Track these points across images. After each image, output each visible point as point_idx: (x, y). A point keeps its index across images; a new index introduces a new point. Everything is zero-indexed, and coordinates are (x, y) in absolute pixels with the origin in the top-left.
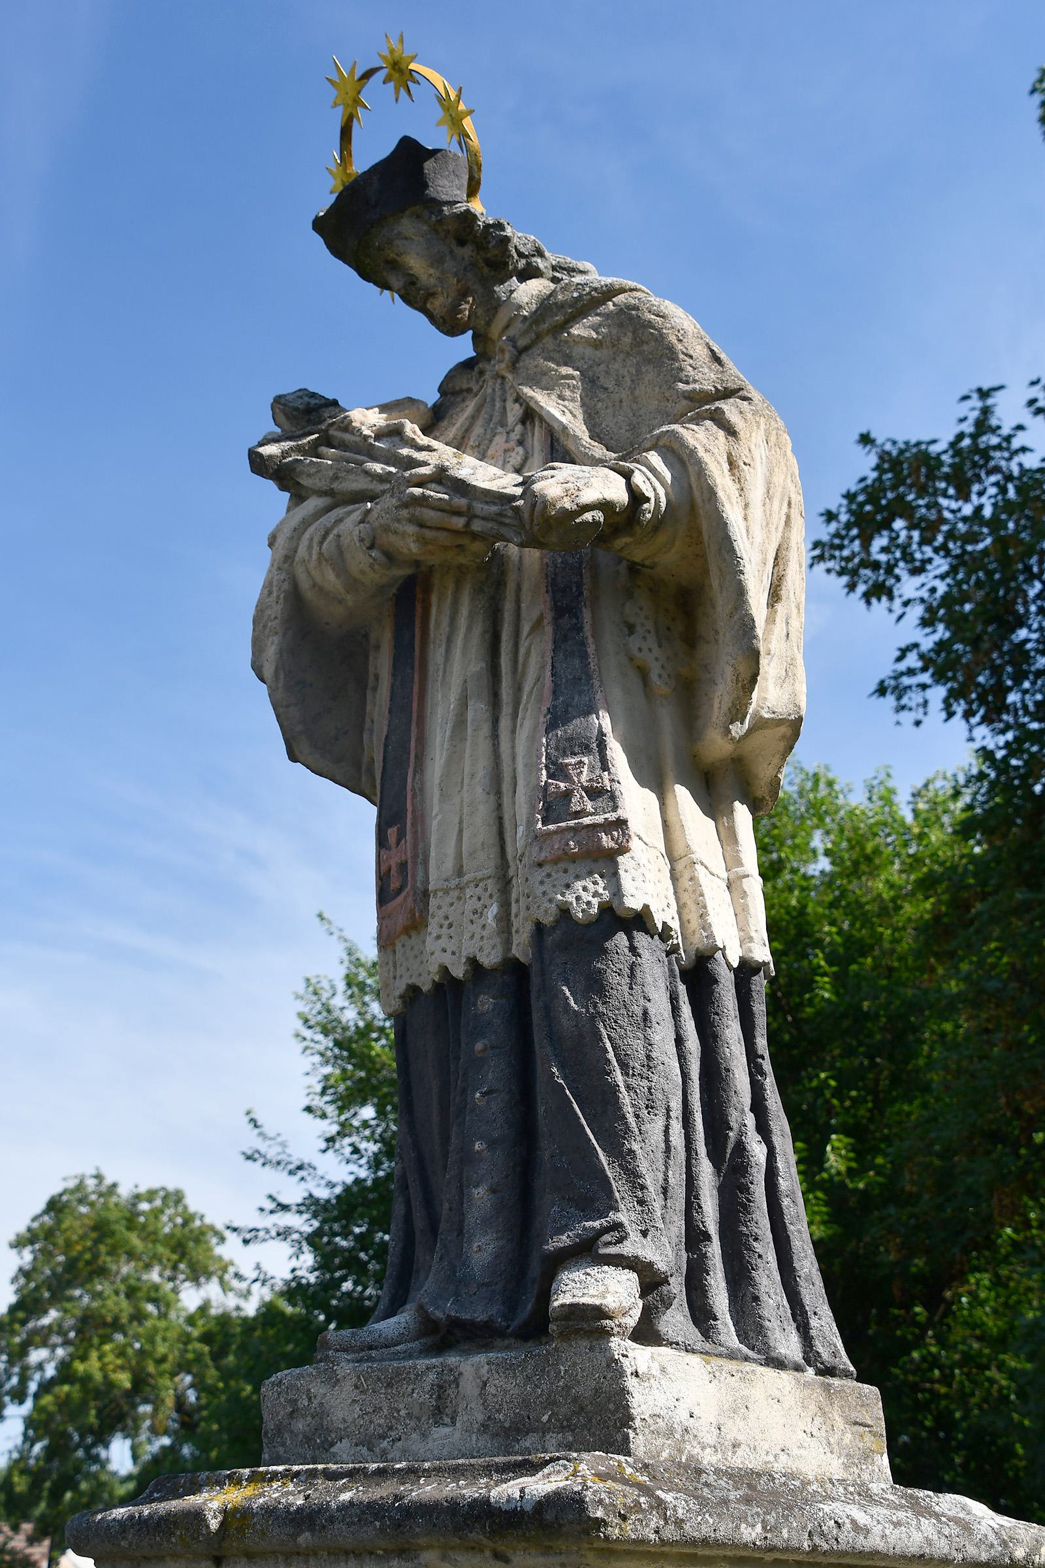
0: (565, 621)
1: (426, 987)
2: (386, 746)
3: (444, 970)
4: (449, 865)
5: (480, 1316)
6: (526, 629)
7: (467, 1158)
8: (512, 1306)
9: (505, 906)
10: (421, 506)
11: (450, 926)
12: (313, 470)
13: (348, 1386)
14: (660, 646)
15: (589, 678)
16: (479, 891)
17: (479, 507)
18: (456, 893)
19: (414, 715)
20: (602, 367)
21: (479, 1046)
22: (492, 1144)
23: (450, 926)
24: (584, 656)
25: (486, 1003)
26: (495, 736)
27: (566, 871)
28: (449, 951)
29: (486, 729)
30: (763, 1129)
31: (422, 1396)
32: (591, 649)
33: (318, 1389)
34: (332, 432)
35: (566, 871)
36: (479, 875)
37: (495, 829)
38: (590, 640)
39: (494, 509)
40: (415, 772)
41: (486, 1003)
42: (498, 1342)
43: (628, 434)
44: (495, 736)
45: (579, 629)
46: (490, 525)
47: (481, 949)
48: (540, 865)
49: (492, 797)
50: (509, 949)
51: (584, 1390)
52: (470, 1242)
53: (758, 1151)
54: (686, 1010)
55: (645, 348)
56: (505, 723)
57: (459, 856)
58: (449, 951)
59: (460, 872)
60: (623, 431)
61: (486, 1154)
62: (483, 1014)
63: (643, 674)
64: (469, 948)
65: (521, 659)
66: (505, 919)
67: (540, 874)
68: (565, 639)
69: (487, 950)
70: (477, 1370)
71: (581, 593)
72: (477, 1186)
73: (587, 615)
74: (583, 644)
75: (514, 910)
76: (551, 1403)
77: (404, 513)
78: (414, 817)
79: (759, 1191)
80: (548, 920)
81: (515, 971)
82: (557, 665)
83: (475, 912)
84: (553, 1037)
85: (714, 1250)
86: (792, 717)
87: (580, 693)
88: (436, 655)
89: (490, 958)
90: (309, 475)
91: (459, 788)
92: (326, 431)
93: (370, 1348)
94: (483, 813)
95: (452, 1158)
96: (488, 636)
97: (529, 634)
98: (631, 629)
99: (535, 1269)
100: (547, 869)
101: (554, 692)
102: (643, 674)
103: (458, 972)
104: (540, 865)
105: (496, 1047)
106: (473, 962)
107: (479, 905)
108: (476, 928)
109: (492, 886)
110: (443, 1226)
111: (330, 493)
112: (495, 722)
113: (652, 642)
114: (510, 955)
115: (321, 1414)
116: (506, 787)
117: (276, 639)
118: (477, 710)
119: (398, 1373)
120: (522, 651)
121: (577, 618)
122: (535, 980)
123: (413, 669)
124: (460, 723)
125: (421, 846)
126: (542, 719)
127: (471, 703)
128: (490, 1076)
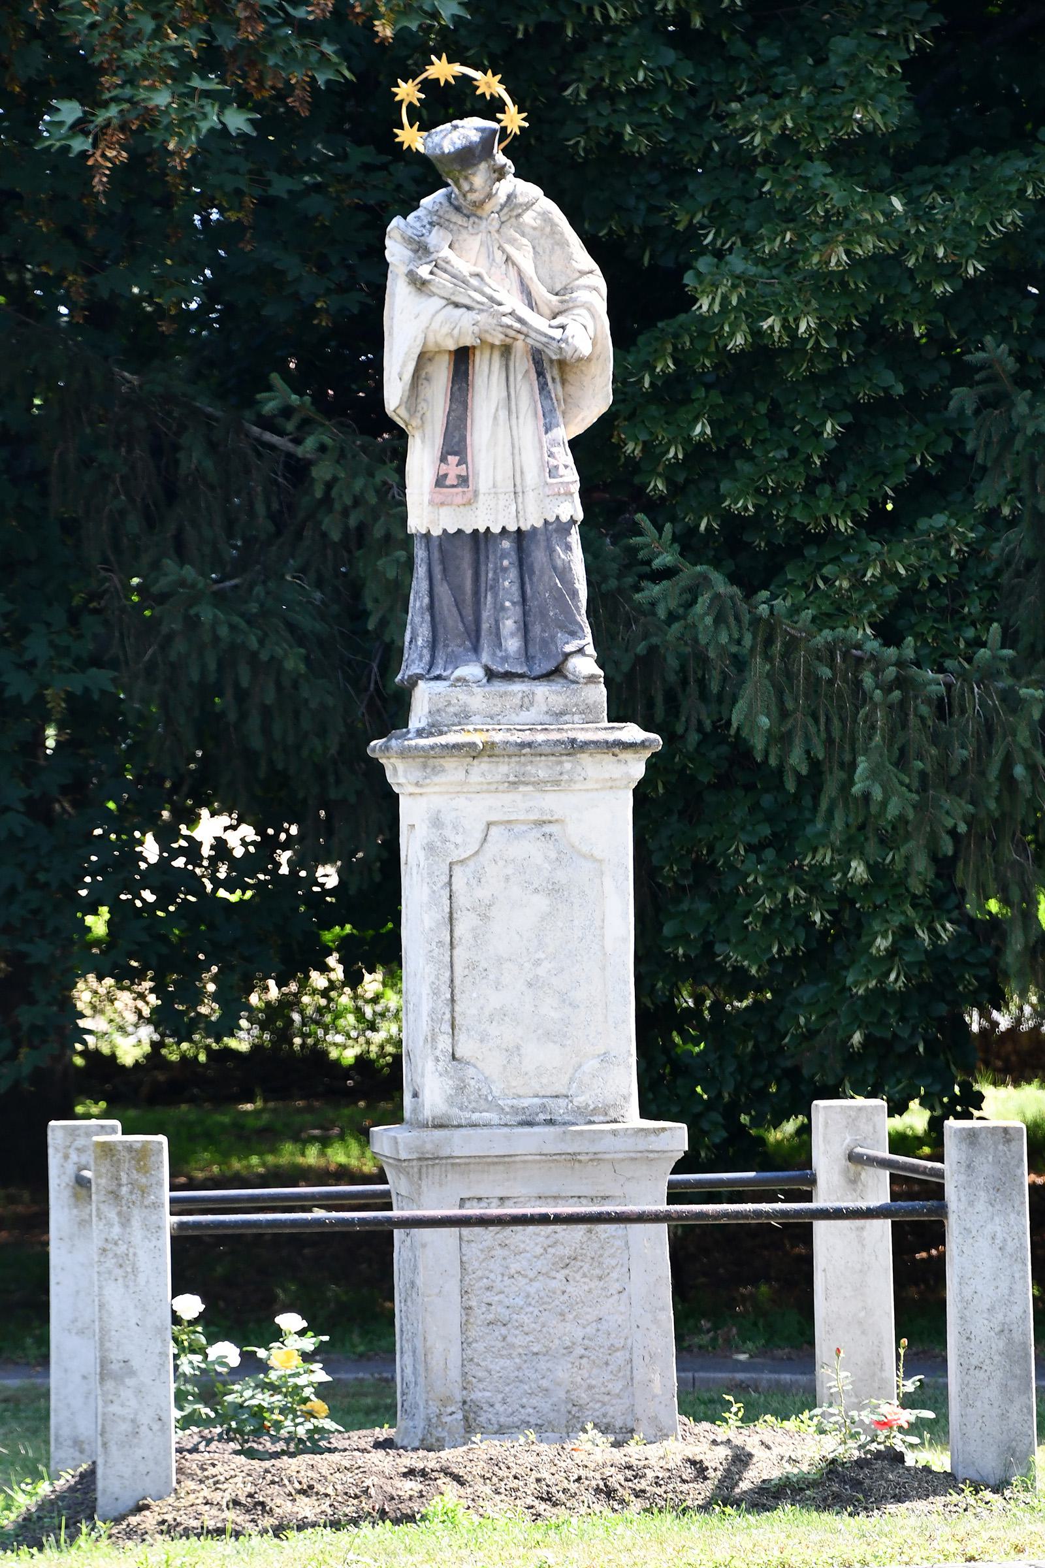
5: (520, 671)
6: (520, 377)
17: (533, 334)
22: (513, 603)
25: (506, 544)
31: (517, 701)
33: (463, 697)
39: (544, 340)
51: (590, 701)
56: (514, 421)
59: (494, 486)
67: (548, 500)
76: (577, 705)
77: (500, 329)
103: (496, 530)
110: (483, 634)
115: (466, 705)
116: (516, 451)
118: (503, 414)
124: (495, 418)
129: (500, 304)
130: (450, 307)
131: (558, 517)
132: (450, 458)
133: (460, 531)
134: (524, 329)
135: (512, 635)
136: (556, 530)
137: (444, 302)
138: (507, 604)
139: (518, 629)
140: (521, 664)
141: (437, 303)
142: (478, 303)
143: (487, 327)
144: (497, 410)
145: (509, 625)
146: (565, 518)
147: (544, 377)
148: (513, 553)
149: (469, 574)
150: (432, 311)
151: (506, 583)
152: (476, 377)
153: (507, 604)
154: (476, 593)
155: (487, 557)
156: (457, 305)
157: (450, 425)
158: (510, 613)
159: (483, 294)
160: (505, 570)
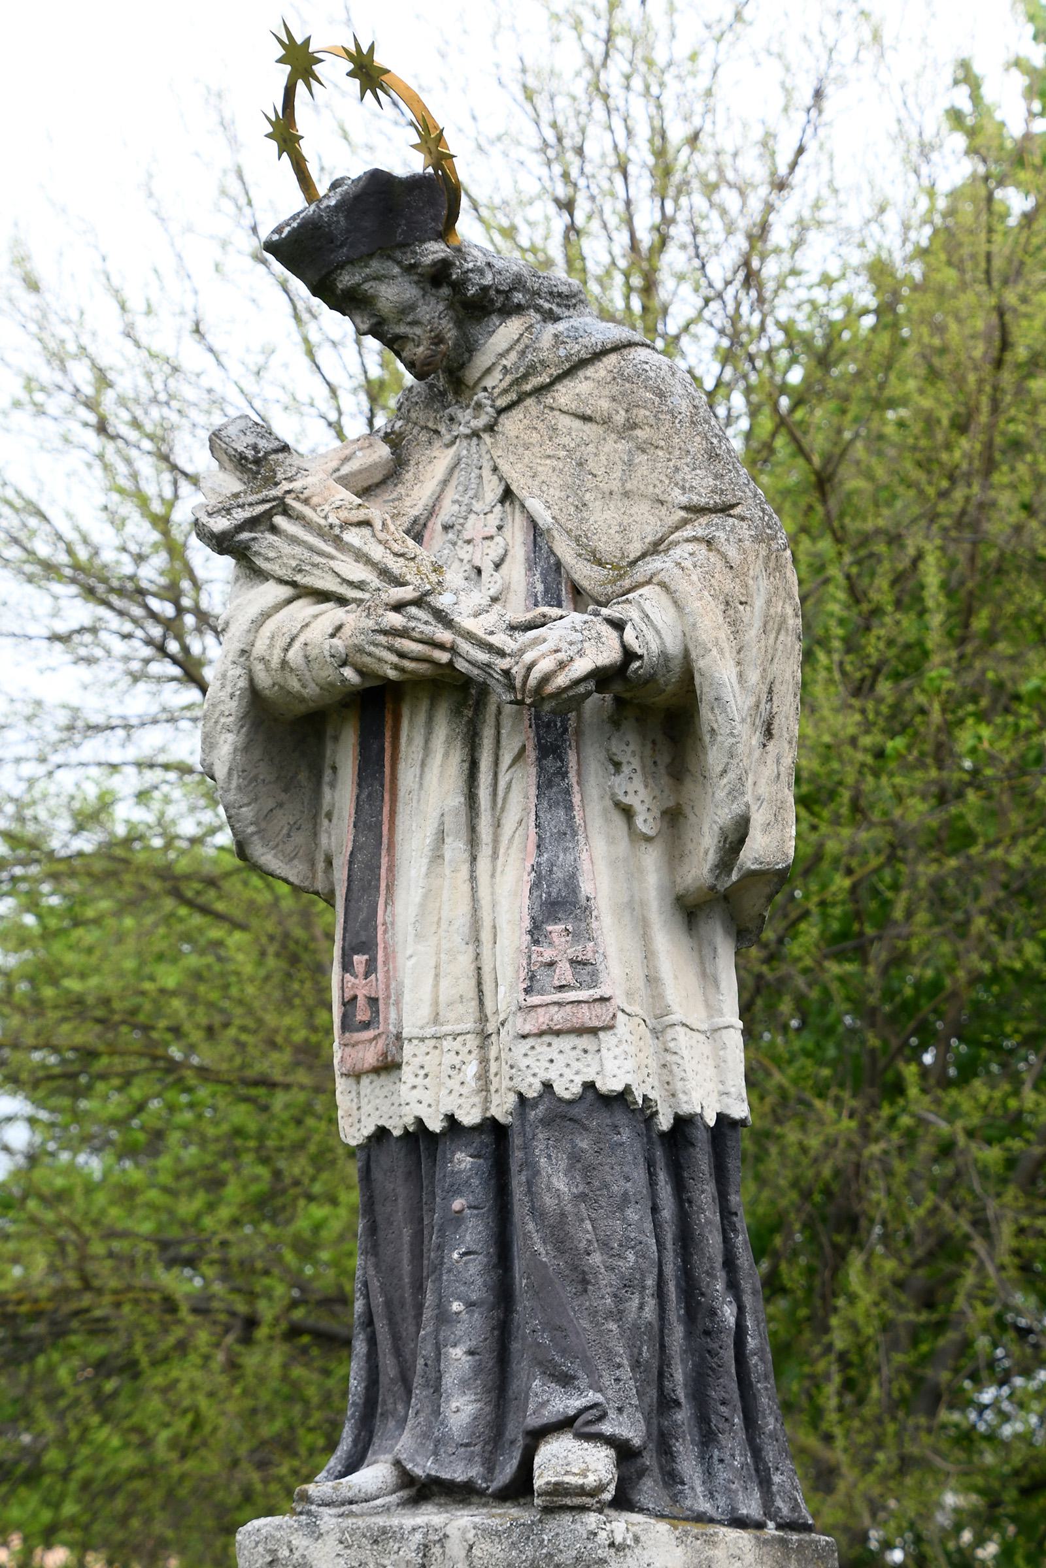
0: (550, 763)
1: (397, 1133)
2: (351, 862)
3: (419, 1121)
4: (425, 1012)
6: (506, 759)
7: (444, 1317)
8: (490, 1468)
9: (484, 1061)
10: (402, 637)
11: (426, 1075)
12: (271, 555)
13: (331, 1542)
14: (646, 786)
15: (575, 833)
16: (457, 1045)
17: (465, 646)
18: (433, 1042)
19: (385, 840)
20: (591, 448)
21: (457, 1204)
22: (470, 1305)
23: (426, 1075)
24: (569, 808)
25: (463, 1160)
26: (473, 878)
27: (550, 1045)
28: (425, 1104)
29: (465, 869)
30: (733, 1286)
32: (576, 799)
34: (289, 500)
35: (550, 1045)
36: (458, 1028)
37: (473, 982)
38: (576, 788)
39: (482, 656)
40: (386, 904)
41: (463, 1160)
42: (475, 1499)
43: (618, 537)
44: (473, 878)
45: (565, 775)
46: (476, 671)
47: (460, 1106)
48: (524, 1037)
49: (471, 948)
50: (487, 1109)
52: (448, 1401)
53: (729, 1313)
54: (662, 1177)
55: (638, 432)
56: (483, 864)
57: (436, 1003)
58: (425, 1104)
59: (436, 1020)
60: (612, 531)
61: (464, 1316)
62: (460, 1172)
63: (627, 812)
64: (449, 1105)
65: (501, 793)
66: (484, 1077)
68: (550, 784)
69: (466, 1107)
70: (464, 1533)
71: (566, 730)
72: (455, 1346)
73: (572, 758)
74: (568, 792)
75: (493, 1070)
77: (382, 639)
78: (386, 955)
79: (729, 1355)
80: (531, 1094)
81: (494, 1130)
82: (541, 814)
83: (453, 1067)
84: (537, 1213)
85: (683, 1415)
86: (780, 866)
87: (565, 850)
88: (407, 776)
89: (469, 1117)
90: (267, 559)
91: (434, 929)
92: (281, 500)
93: (351, 1503)
94: (465, 961)
95: (428, 1314)
96: (466, 765)
97: (510, 767)
98: (617, 765)
99: (515, 1431)
100: (531, 1041)
101: (538, 847)
102: (627, 812)
103: (435, 1125)
104: (524, 1037)
105: (475, 1208)
106: (451, 1119)
107: (457, 1061)
108: (454, 1084)
109: (472, 1042)
110: (417, 1381)
111: (293, 584)
112: (474, 859)
113: (638, 783)
114: (488, 1115)
116: (486, 936)
117: (230, 737)
118: (455, 848)
119: (384, 1531)
120: (502, 784)
121: (562, 761)
122: (517, 1141)
123: (382, 786)
124: (437, 857)
125: (393, 985)
126: (526, 878)
127: (448, 840)
128: (468, 1238)
129: (399, 582)
130: (303, 609)
131: (548, 1086)
132: (356, 957)
133: (382, 1133)
134: (445, 636)
135: (464, 1384)
136: (547, 1122)
137: (285, 592)
138: (456, 1306)
139: (477, 1370)
140: (470, 1460)
141: (273, 592)
142: (351, 584)
143: (360, 640)
144: (441, 836)
145: (457, 1355)
146: (568, 1087)
147: (561, 758)
148: (475, 1182)
149: (407, 1233)
150: (253, 611)
151: (455, 1256)
152: (402, 766)
153: (456, 1306)
154: (419, 1288)
155: (433, 1194)
156: (323, 596)
157: (356, 885)
158: (460, 1329)
159: (368, 561)
160: (457, 1219)
